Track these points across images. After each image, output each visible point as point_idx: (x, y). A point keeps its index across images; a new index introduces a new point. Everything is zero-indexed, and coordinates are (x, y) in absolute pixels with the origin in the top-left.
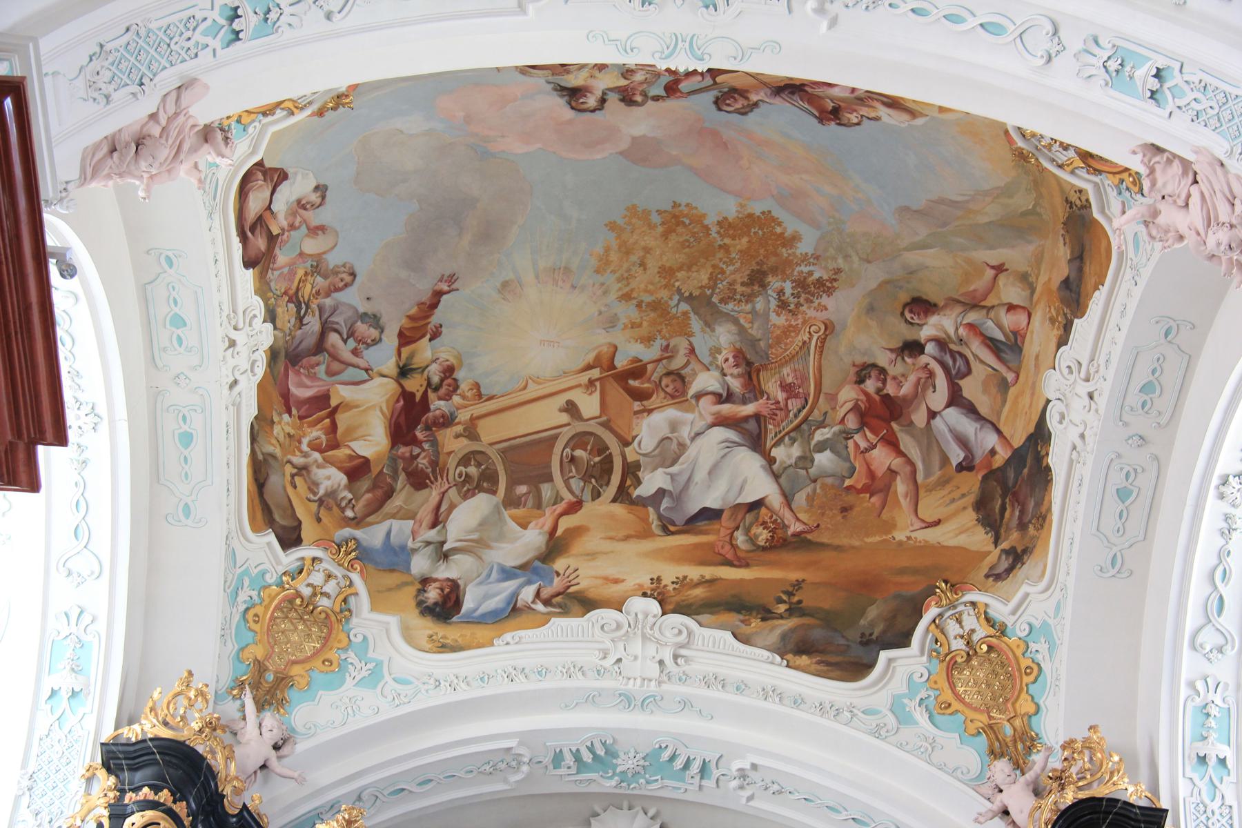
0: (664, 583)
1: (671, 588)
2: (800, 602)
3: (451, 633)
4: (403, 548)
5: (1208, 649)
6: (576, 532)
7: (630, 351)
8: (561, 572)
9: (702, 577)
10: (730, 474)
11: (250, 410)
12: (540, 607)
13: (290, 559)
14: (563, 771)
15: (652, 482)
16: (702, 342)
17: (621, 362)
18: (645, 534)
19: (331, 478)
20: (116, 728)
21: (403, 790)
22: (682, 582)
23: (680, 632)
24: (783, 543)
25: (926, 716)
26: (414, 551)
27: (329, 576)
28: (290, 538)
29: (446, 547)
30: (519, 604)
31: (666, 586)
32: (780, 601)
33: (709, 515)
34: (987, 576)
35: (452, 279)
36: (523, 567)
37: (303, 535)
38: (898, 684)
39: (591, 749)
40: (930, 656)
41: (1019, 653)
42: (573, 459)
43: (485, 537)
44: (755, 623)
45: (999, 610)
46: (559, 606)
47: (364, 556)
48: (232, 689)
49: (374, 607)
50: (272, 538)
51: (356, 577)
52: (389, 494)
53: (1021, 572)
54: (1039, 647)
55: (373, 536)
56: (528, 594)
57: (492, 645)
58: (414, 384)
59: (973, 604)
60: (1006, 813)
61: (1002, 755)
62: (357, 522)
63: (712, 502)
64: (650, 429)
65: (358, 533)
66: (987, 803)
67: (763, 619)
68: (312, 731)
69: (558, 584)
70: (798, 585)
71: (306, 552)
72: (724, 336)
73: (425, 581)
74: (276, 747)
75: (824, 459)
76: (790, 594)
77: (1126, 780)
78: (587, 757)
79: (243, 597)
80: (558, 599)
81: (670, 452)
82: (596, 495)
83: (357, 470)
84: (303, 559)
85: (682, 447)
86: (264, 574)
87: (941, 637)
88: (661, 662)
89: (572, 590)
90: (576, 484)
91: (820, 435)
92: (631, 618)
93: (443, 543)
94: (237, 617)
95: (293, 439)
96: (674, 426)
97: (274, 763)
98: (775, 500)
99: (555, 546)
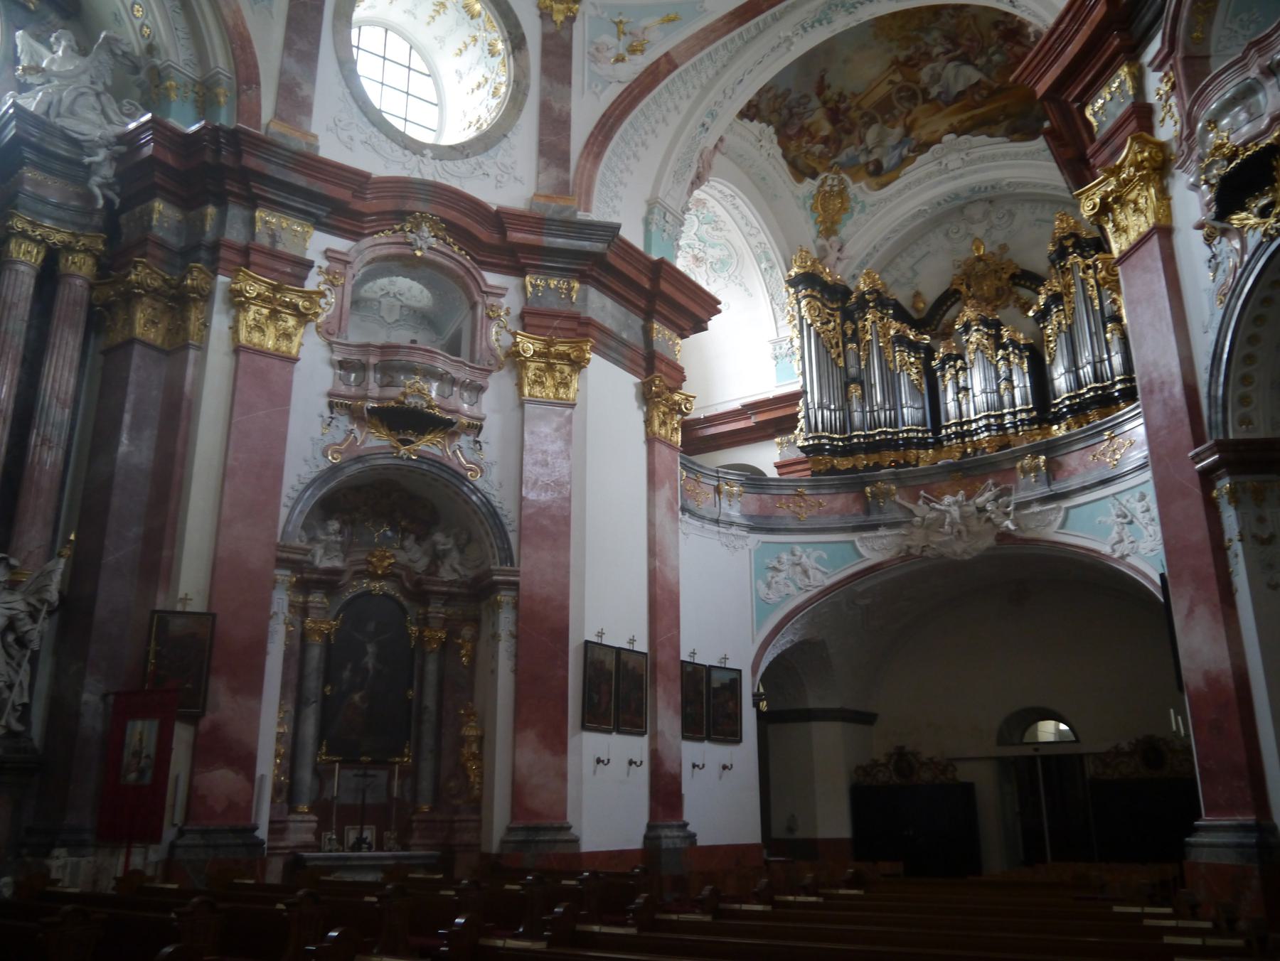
3: (884, 179)
6: (914, 121)
7: (902, 55)
10: (963, 76)
11: (778, 151)
13: (817, 182)
15: (934, 91)
16: (929, 39)
17: (901, 58)
18: (939, 110)
19: (818, 148)
22: (961, 122)
24: (993, 93)
28: (814, 175)
33: (961, 94)
35: (825, 70)
42: (901, 98)
43: (881, 139)
47: (843, 167)
49: (854, 182)
50: (809, 180)
51: (843, 175)
52: (840, 141)
55: (842, 157)
56: (905, 152)
57: (897, 177)
58: (830, 105)
62: (835, 156)
63: (960, 87)
64: (925, 74)
65: (836, 160)
69: (914, 143)
71: (822, 176)
72: (936, 34)
73: (867, 164)
75: (996, 58)
79: (808, 205)
81: (936, 78)
82: (916, 105)
83: (825, 140)
85: (940, 75)
90: (906, 105)
91: (990, 51)
95: (799, 147)
96: (933, 69)
98: (984, 79)
99: (908, 130)
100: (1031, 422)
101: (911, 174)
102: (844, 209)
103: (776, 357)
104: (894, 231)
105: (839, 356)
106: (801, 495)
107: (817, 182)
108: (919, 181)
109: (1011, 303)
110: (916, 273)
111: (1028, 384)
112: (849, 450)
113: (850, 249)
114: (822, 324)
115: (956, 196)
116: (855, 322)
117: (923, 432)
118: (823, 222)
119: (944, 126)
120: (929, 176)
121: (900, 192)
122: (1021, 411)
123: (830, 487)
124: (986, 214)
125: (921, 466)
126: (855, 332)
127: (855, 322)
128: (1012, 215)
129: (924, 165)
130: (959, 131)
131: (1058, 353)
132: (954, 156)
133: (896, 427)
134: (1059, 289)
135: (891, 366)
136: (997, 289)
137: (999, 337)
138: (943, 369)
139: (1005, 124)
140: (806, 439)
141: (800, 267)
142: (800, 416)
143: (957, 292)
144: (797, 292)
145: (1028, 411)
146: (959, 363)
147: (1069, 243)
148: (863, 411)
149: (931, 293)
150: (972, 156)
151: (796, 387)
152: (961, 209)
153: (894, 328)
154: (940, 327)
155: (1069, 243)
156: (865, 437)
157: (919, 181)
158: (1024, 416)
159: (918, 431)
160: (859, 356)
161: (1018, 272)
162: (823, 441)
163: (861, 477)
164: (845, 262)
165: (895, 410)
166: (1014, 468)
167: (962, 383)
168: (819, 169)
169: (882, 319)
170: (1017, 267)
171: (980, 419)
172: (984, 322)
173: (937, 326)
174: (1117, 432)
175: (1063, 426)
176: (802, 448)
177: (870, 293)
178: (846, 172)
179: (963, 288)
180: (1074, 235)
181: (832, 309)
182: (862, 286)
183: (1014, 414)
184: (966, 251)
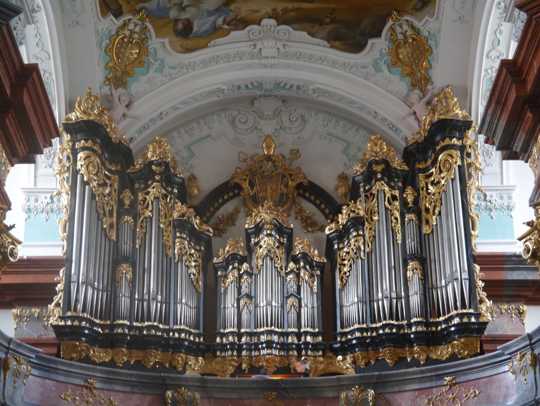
0: (277, 10)
1: (280, 13)
2: (335, 17)
3: (190, 43)
4: (165, 8)
5: (493, 58)
8: (233, 10)
9: (294, 7)
12: (226, 27)
14: (241, 91)
20: (66, 114)
21: (177, 108)
22: (285, 10)
23: (285, 34)
25: (387, 68)
26: (170, 8)
27: (136, 25)
28: (118, 14)
29: (183, 5)
30: (217, 26)
31: (278, 12)
32: (327, 17)
34: (413, 9)
36: (217, 10)
37: (123, 10)
38: (376, 54)
39: (252, 84)
40: (389, 41)
41: (424, 42)
44: (317, 27)
45: (416, 23)
46: (234, 25)
47: (150, 14)
48: (105, 82)
49: (157, 36)
50: (112, 17)
51: (148, 25)
53: (427, 10)
54: (431, 43)
56: (220, 21)
57: (206, 46)
59: (407, 21)
60: (415, 113)
61: (416, 85)
65: (146, 5)
66: (409, 109)
67: (320, 25)
68: (139, 95)
70: (334, 10)
71: (126, 17)
73: (176, 21)
74: (127, 106)
76: (331, 14)
77: (458, 109)
78: (250, 86)
79: (104, 45)
80: (233, 22)
84: (125, 21)
86: (110, 31)
87: (393, 34)
88: (278, 49)
89: (239, 17)
92: (265, 28)
93: (182, 3)
94: (103, 53)
97: (128, 113)
100: (315, 347)
101: (221, 47)
102: (139, 61)
103: (29, 210)
104: (185, 103)
105: (111, 226)
106: (90, 388)
107: (119, 23)
108: (228, 58)
109: (293, 213)
110: (192, 155)
111: (315, 305)
112: (110, 341)
113: (137, 109)
114: (99, 185)
115: (260, 85)
116: (134, 193)
117: (195, 335)
118: (113, 69)
119: (268, 9)
120: (240, 55)
121: (205, 63)
122: (306, 333)
123: (125, 383)
124: (277, 113)
125: (188, 373)
126: (134, 203)
127: (134, 193)
128: (304, 121)
129: (236, 42)
130: (282, 19)
131: (352, 280)
132: (272, 43)
133: (167, 322)
134: (362, 213)
135: (170, 253)
136: (282, 195)
137: (289, 248)
138: (226, 268)
139: (329, 28)
140: (61, 318)
141: (84, 112)
142: (60, 287)
143: (239, 187)
144: (73, 141)
145: (314, 335)
146: (245, 266)
147: (379, 168)
148: (132, 298)
149: (208, 178)
150: (287, 49)
151: (58, 252)
152: (252, 100)
153: (179, 209)
154: (213, 221)
155: (379, 168)
156: (130, 328)
157: (228, 58)
158: (309, 339)
159: (190, 333)
160: (134, 231)
161: (305, 182)
162: (84, 323)
163: (163, 378)
164: (128, 120)
165: (168, 303)
166: (338, 398)
167: (245, 290)
168: (125, 8)
169: (165, 196)
170: (305, 177)
171: (262, 333)
172: (280, 230)
173: (209, 219)
174: (463, 378)
175: (349, 359)
176: (56, 328)
177: (159, 164)
178: (151, 22)
179: (246, 185)
180: (386, 162)
181: (110, 171)
182: (149, 155)
183: (299, 335)
184: (252, 145)
